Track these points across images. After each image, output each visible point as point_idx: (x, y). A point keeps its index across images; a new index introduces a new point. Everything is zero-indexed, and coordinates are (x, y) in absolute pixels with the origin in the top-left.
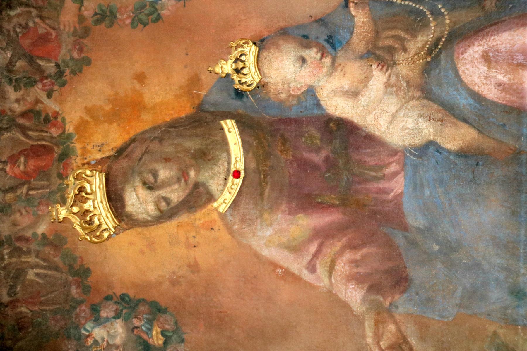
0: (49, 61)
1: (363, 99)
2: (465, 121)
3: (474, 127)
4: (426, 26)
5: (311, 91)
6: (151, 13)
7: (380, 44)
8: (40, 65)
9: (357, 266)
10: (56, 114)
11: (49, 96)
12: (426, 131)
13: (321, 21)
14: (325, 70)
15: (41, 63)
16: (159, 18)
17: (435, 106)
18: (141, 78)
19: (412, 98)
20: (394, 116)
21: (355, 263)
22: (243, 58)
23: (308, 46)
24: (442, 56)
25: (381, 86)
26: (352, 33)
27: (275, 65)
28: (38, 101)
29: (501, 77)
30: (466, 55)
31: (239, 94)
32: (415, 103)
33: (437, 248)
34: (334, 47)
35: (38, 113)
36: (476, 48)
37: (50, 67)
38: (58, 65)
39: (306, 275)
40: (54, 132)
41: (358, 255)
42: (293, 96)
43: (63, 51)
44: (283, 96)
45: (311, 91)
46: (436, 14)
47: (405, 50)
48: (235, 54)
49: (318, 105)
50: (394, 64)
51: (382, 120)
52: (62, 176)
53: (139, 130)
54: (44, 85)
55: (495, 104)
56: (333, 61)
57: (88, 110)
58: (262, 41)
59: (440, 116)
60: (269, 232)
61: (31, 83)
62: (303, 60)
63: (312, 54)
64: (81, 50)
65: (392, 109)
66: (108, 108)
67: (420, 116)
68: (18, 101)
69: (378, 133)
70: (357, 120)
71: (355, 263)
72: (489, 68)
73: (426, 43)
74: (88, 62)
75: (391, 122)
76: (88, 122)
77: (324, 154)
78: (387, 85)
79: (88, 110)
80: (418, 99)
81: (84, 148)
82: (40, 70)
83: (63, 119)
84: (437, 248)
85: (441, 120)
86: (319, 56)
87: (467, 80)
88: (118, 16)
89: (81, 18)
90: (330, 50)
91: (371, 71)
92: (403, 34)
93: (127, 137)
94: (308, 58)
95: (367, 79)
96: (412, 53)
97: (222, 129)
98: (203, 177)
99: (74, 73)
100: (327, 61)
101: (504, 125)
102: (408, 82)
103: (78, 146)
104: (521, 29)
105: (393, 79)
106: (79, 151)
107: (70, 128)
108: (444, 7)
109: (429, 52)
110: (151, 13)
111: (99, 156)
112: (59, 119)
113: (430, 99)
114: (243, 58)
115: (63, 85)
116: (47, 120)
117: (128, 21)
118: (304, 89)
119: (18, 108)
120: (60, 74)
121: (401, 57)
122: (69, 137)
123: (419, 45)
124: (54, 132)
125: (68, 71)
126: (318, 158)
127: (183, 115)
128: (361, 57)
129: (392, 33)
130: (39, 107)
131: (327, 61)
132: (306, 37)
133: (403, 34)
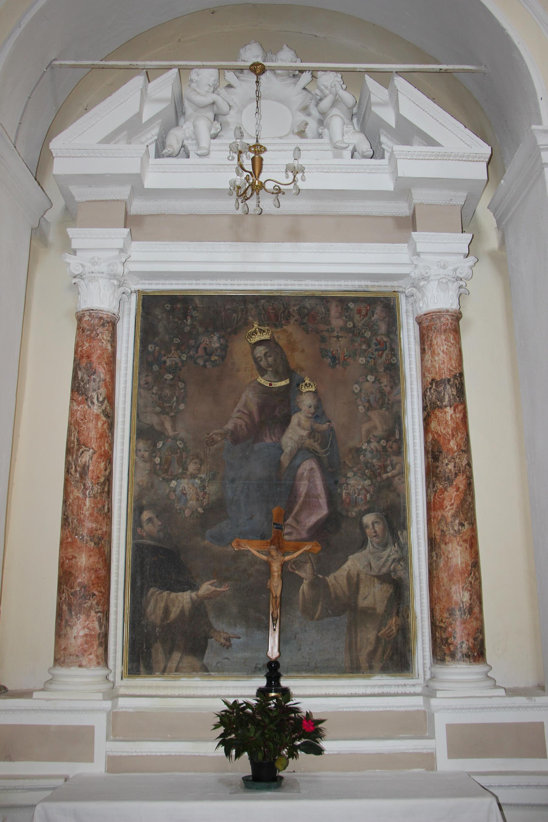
0: (307, 320)
1: (297, 428)
2: (291, 462)
3: (288, 466)
4: (322, 449)
5: (300, 410)
6: (324, 355)
7: (316, 434)
8: (305, 317)
9: (240, 427)
10: (289, 323)
11: (295, 320)
12: (287, 449)
13: (323, 413)
14: (307, 415)
15: (306, 318)
16: (323, 357)
17: (295, 452)
18: (303, 351)
19: (298, 445)
20: (292, 439)
21: (241, 426)
22: (310, 386)
23: (315, 409)
24: (312, 454)
25: (302, 434)
26: (320, 424)
27: (308, 397)
28: (293, 316)
29: (305, 474)
30: (312, 462)
31: (298, 385)
32: (296, 446)
33: (247, 454)
34: (315, 417)
35: (290, 317)
36: (315, 465)
37: (305, 321)
38: (306, 323)
39: (236, 409)
40: (283, 322)
41: (243, 427)
42: (298, 404)
43: (311, 325)
44: (298, 400)
45: (300, 410)
46: (327, 452)
47: (314, 442)
48: (312, 384)
49: (295, 412)
50: (309, 438)
51: (290, 434)
52: (268, 325)
53: (285, 350)
54: (299, 319)
55: (296, 472)
56: (310, 417)
57: (291, 333)
58: (317, 393)
59: (292, 454)
60: (251, 396)
61: (300, 314)
62: (310, 407)
63: (312, 410)
64: (311, 331)
65: (294, 438)
66: (292, 340)
67: (292, 447)
68: (293, 310)
69: (286, 433)
70: (290, 426)
71: (241, 426)
72: (308, 470)
73: (317, 449)
74: (308, 333)
75: (290, 438)
76: (287, 333)
77: (278, 415)
78: (302, 436)
79: (291, 333)
80: (298, 447)
81: (278, 332)
82: (304, 317)
83: (288, 325)
84: (247, 454)
85: (291, 455)
86: (312, 412)
87: (304, 463)
88: (323, 344)
89: (322, 331)
90: (314, 416)
91: (307, 430)
92: (319, 441)
93: (282, 346)
94: (310, 409)
95: (304, 429)
96: (313, 444)
97: (286, 379)
98: (269, 373)
99: (304, 328)
100: (310, 415)
101: (289, 475)
102: (303, 443)
103: (279, 330)
104: (321, 480)
105: (304, 438)
106: (277, 330)
107: (285, 327)
108: (329, 454)
109: (313, 450)
110: (324, 355)
111: (276, 337)
112: (288, 324)
113: (297, 451)
114: (310, 386)
115: (300, 325)
116: (287, 320)
117: (322, 347)
118: (300, 407)
119: (291, 310)
120: (303, 324)
121: (312, 440)
122: (282, 327)
123: (316, 447)
124: (283, 322)
125: (304, 326)
126: (277, 412)
127: (290, 366)
128: (312, 427)
129: (320, 437)
130: (292, 317)
131: (310, 415)
132: (318, 408)
133: (319, 441)
